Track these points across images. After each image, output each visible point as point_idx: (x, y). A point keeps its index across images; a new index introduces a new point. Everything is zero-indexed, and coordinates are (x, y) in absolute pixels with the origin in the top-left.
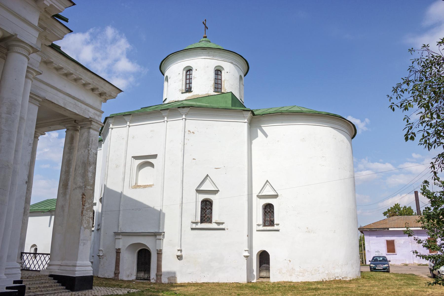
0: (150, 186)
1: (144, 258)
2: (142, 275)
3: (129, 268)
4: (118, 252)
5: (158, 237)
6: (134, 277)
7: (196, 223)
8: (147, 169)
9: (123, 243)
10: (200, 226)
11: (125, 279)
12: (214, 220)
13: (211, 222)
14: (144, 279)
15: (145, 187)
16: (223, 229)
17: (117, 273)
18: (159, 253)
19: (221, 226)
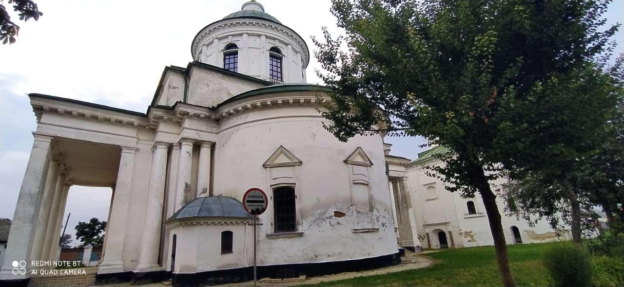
0: (437, 198)
1: (442, 236)
2: (443, 245)
3: (435, 242)
4: (428, 234)
5: (447, 225)
6: (439, 247)
7: (467, 215)
8: (432, 189)
9: (428, 230)
10: (469, 216)
11: (434, 248)
12: (477, 212)
13: (475, 213)
14: (445, 248)
15: (433, 199)
16: (484, 216)
17: (429, 245)
18: (450, 233)
19: (482, 215)
